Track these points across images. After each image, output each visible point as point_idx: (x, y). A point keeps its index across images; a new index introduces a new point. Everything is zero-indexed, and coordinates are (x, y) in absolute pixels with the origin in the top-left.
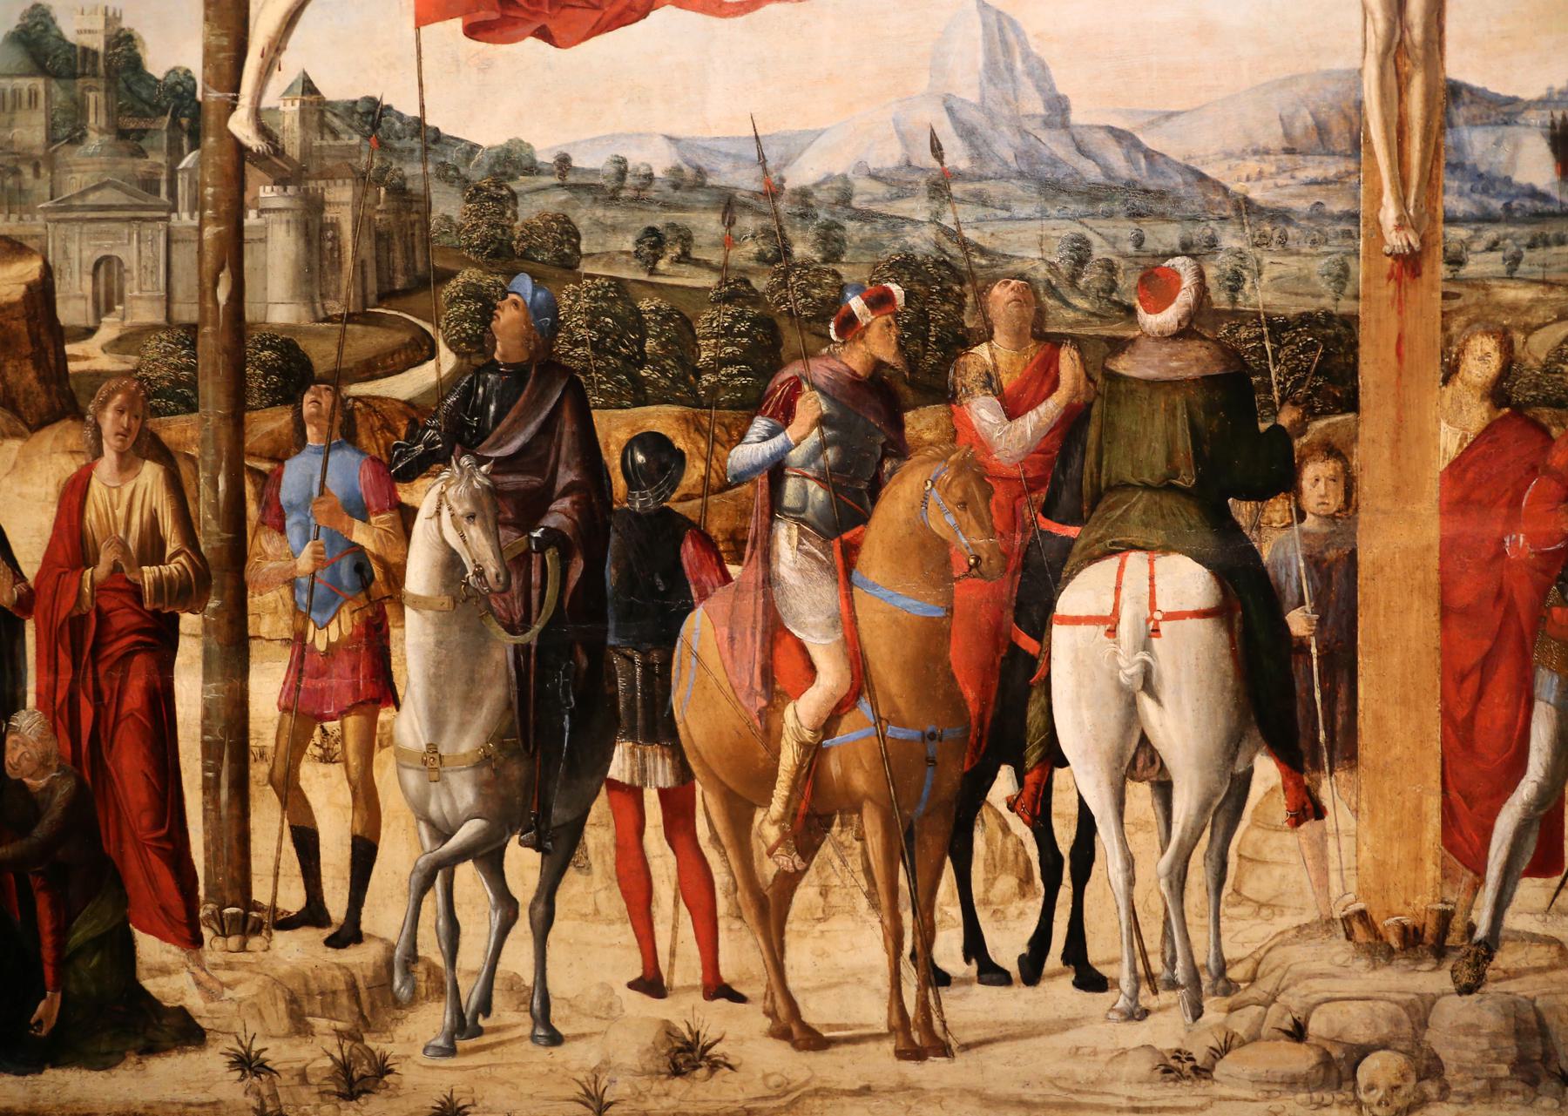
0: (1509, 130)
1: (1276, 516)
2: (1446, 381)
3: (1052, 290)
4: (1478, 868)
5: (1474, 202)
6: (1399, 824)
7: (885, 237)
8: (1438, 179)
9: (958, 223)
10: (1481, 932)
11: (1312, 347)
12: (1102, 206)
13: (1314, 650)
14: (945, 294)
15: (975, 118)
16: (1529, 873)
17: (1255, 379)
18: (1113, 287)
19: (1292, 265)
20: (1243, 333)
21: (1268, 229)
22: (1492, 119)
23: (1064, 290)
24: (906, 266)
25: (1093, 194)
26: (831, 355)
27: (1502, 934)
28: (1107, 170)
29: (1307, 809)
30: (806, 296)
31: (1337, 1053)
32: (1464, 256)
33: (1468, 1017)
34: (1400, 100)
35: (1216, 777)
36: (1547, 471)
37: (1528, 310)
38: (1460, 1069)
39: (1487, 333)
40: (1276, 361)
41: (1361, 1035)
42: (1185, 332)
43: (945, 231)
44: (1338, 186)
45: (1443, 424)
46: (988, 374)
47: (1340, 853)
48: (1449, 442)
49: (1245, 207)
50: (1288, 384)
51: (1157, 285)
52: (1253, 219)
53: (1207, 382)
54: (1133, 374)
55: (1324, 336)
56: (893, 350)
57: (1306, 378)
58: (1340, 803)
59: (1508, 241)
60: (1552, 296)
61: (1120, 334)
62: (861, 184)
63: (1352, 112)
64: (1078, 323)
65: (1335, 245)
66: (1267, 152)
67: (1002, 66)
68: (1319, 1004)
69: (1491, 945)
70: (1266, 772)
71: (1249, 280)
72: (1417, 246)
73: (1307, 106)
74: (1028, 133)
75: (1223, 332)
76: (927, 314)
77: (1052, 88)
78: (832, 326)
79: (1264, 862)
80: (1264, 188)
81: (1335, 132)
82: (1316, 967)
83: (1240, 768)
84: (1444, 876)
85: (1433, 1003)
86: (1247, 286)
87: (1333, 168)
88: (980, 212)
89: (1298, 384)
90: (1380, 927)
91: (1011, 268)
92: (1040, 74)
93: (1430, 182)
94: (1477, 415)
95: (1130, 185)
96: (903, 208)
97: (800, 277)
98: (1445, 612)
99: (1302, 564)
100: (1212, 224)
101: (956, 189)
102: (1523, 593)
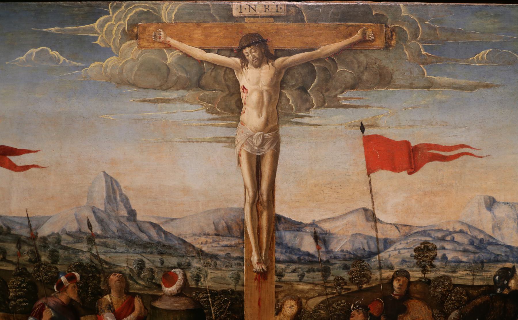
0: (299, 233)
3: (131, 278)
5: (287, 256)
7: (73, 256)
8: (273, 247)
9: (97, 253)
11: (227, 301)
12: (148, 250)
14: (94, 277)
15: (103, 216)
17: (205, 311)
18: (153, 278)
19: (219, 273)
20: (201, 296)
21: (210, 261)
22: (293, 229)
23: (135, 278)
24: (80, 266)
25: (145, 246)
26: (55, 296)
28: (150, 237)
30: (46, 275)
32: (283, 274)
34: (259, 220)
37: (307, 292)
39: (292, 299)
40: (213, 305)
42: (180, 294)
43: (93, 255)
44: (236, 248)
46: (109, 305)
49: (201, 253)
50: (218, 313)
51: (170, 279)
53: (188, 311)
54: (161, 307)
55: (231, 298)
56: (76, 296)
57: (224, 311)
59: (299, 270)
60: (316, 288)
61: (156, 294)
62: (64, 237)
63: (240, 223)
64: (141, 289)
65: (234, 268)
66: (209, 235)
67: (112, 198)
71: (203, 278)
72: (265, 269)
73: (223, 220)
74: (122, 223)
75: (194, 295)
76: (88, 284)
77: (130, 207)
78: (55, 286)
80: (208, 247)
81: (234, 229)
86: (202, 280)
87: (233, 242)
88: (105, 249)
89: (221, 313)
91: (116, 269)
92: (126, 201)
93: (270, 248)
95: (159, 243)
96: (78, 246)
97: (44, 268)
100: (189, 258)
101: (97, 241)
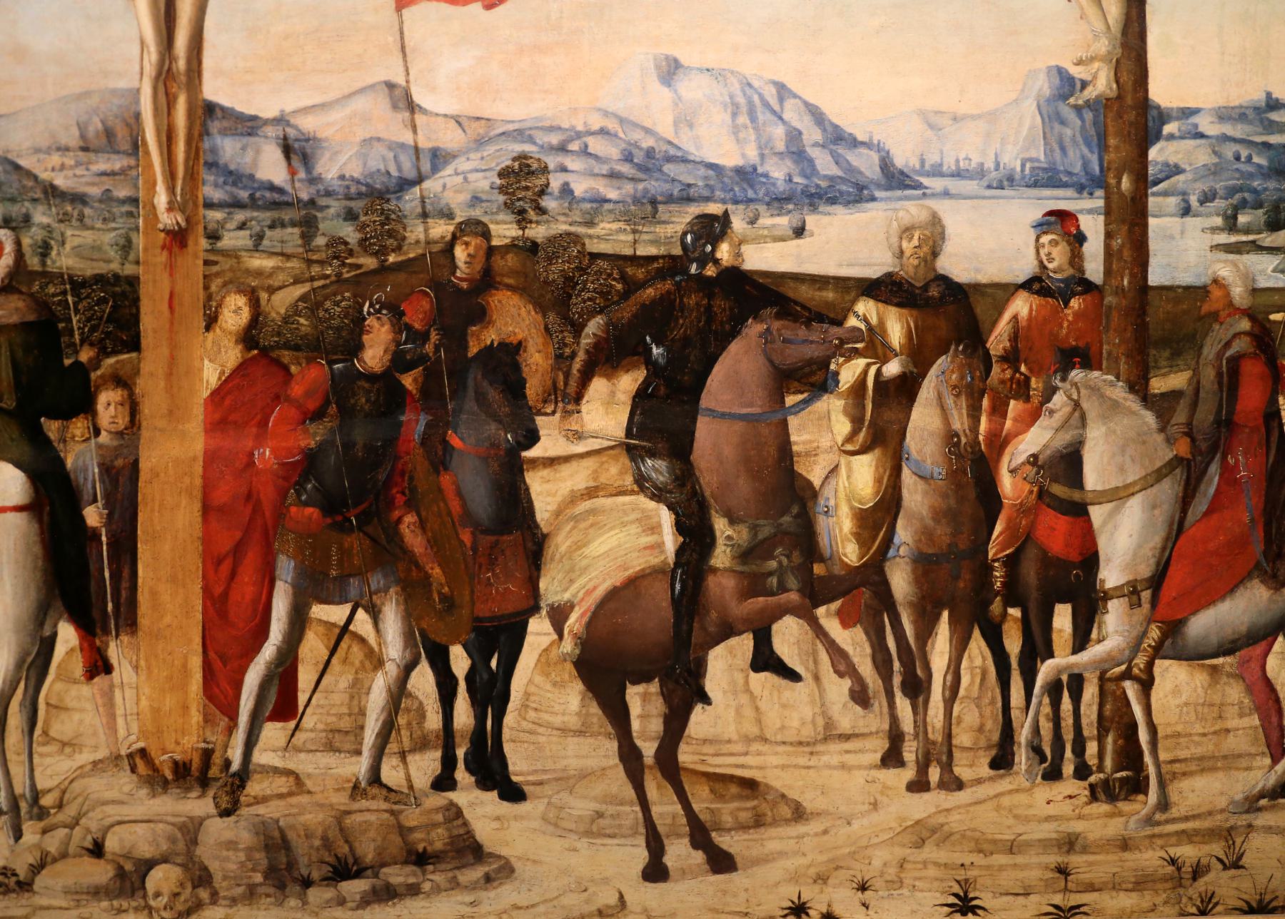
1: (78, 432)
2: (208, 328)
4: (233, 716)
6: (170, 678)
10: (235, 766)
11: (103, 301)
13: (104, 539)
16: (271, 719)
17: (61, 325)
19: (88, 237)
20: (51, 290)
21: (69, 208)
27: (251, 767)
29: (98, 666)
31: (129, 867)
33: (228, 835)
34: (169, 114)
35: (29, 640)
36: (288, 399)
37: (271, 275)
38: (225, 878)
39: (239, 292)
41: (146, 851)
45: (206, 362)
47: (124, 701)
48: (211, 375)
49: (51, 192)
52: (58, 201)
53: (24, 326)
58: (124, 662)
60: (288, 265)
65: (120, 222)
68: (112, 826)
69: (243, 777)
70: (67, 636)
72: (183, 224)
75: (36, 288)
79: (66, 709)
82: (109, 795)
83: (47, 632)
84: (206, 721)
85: (201, 824)
89: (94, 329)
90: (157, 762)
94: (233, 356)
98: (206, 509)
99: (96, 470)
100: (26, 204)
102: (267, 495)
